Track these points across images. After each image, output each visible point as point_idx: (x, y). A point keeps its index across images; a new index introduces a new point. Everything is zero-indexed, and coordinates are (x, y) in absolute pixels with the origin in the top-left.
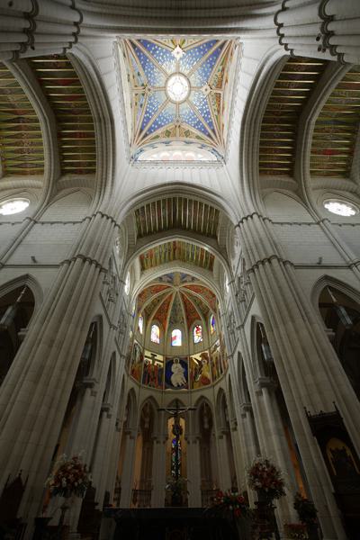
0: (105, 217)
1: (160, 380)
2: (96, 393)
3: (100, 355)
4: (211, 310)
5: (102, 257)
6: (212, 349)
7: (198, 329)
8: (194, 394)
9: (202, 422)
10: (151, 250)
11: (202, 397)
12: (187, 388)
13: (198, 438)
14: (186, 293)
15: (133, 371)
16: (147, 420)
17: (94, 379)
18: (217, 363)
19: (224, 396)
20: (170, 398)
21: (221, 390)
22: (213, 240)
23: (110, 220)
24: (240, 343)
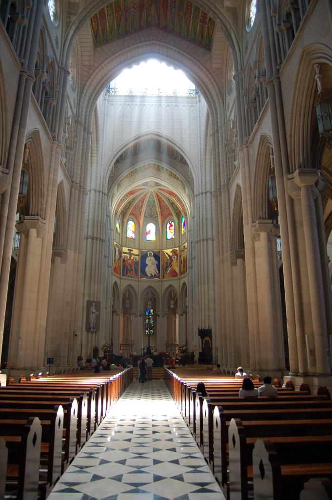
1: (136, 271)
7: (171, 225)
9: (169, 304)
12: (159, 278)
13: (165, 314)
20: (146, 285)
21: (184, 283)
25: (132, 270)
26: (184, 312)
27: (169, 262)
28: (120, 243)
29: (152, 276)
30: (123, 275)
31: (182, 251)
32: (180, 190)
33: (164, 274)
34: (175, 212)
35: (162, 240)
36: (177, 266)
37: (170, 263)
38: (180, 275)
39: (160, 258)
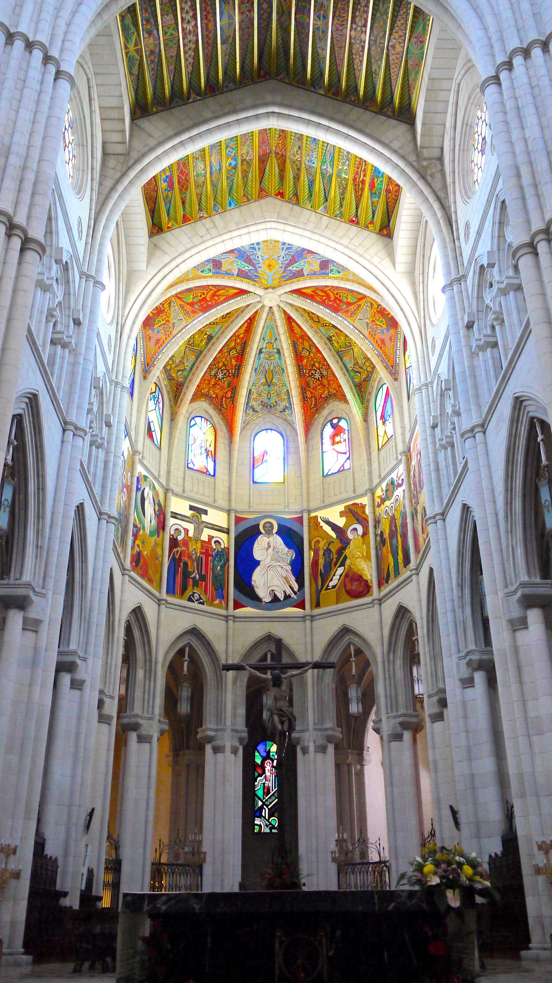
0: (19, 44)
2: (38, 622)
3: (40, 516)
4: (382, 372)
5: (26, 197)
6: (379, 493)
7: (337, 430)
8: (317, 623)
10: (183, 164)
11: (345, 631)
12: (301, 605)
14: (297, 309)
15: (137, 559)
16: (185, 693)
17: (28, 585)
18: (392, 534)
19: (411, 631)
22: (403, 128)
23: (38, 54)
24: (470, 477)
25: (203, 578)
26: (405, 726)
27: (334, 549)
28: (163, 480)
29: (275, 599)
30: (171, 591)
31: (383, 501)
32: (376, 260)
33: (318, 592)
34: (353, 379)
35: (308, 482)
36: (367, 558)
37: (340, 551)
38: (380, 585)
39: (302, 539)
